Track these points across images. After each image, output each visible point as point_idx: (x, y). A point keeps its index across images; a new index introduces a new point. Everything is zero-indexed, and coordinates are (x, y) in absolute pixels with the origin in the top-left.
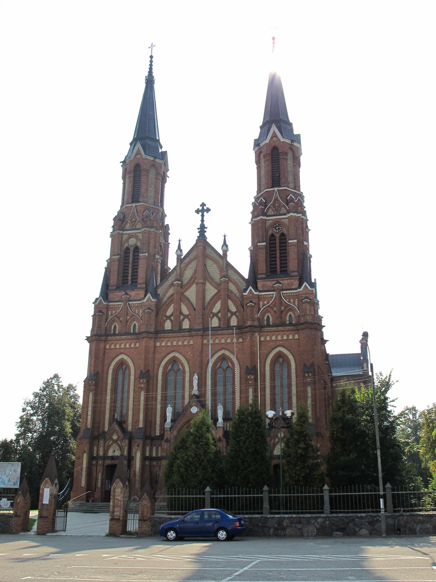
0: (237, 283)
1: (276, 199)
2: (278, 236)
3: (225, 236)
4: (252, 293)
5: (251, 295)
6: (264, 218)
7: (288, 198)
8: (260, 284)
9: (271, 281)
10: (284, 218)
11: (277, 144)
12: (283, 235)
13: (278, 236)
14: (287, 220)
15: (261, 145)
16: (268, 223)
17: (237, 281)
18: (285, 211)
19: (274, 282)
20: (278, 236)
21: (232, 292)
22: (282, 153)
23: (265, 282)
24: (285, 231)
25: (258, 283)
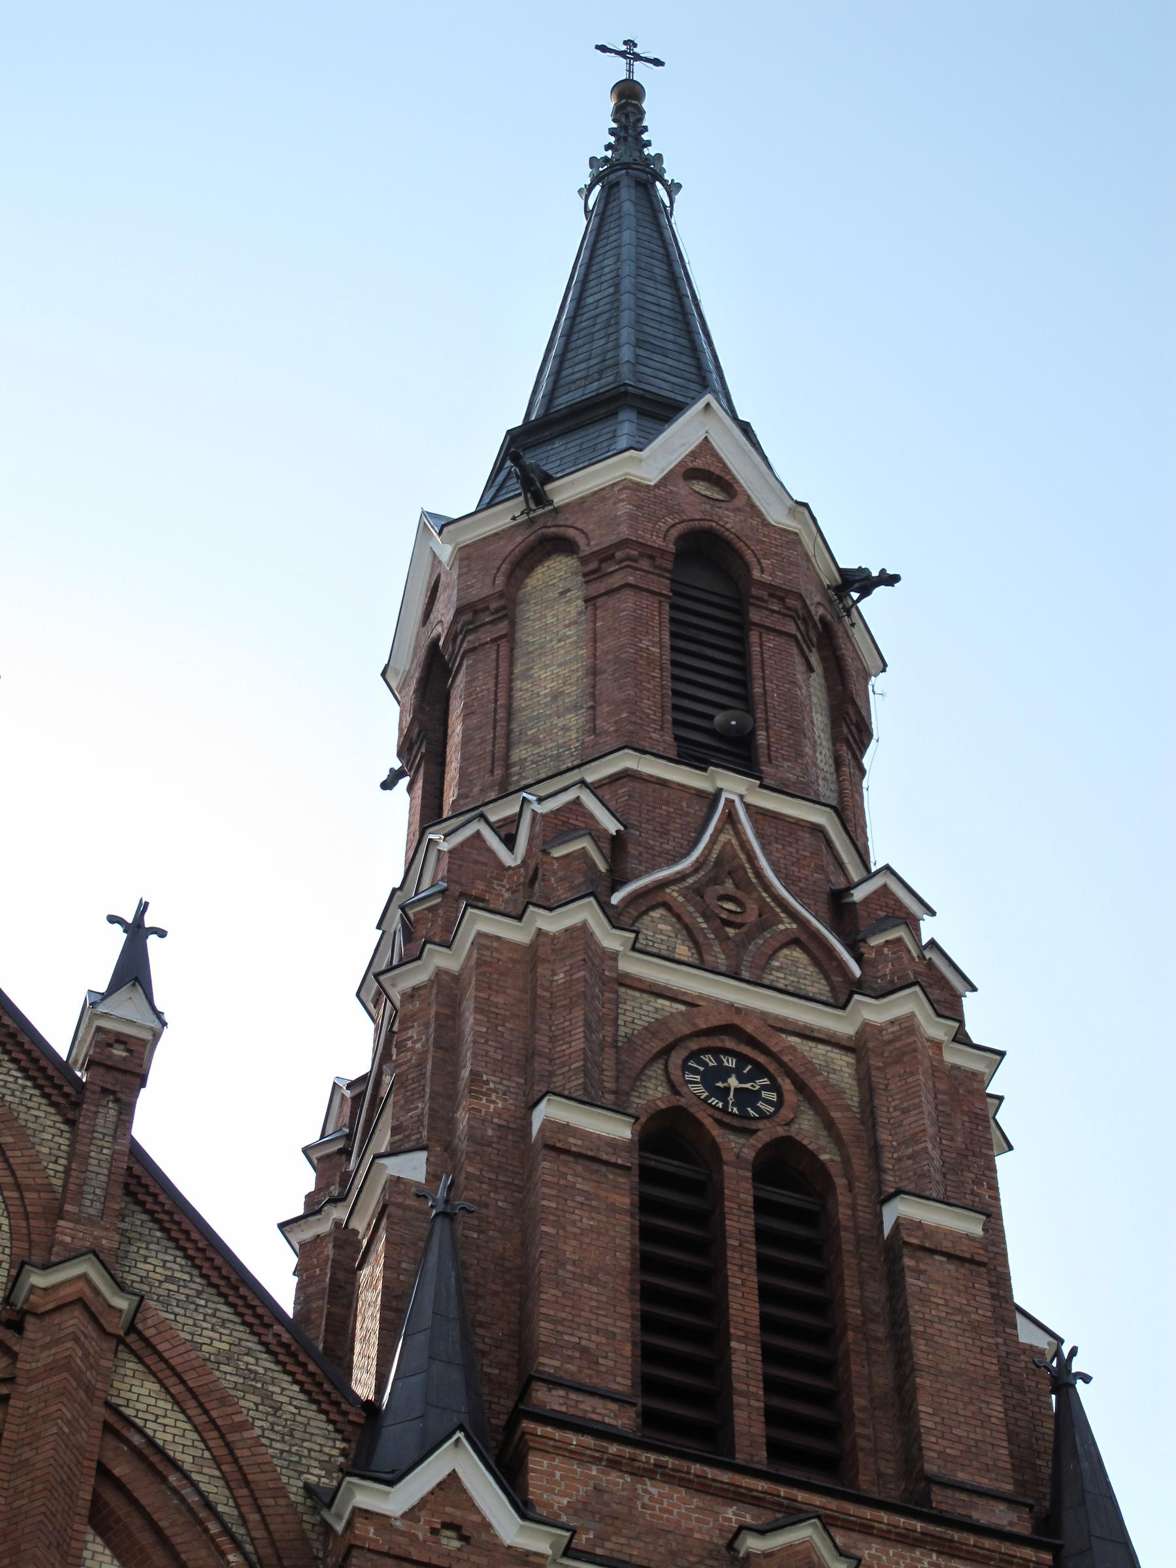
0: (224, 1400)
1: (728, 868)
2: (738, 1150)
3: (137, 933)
4: (469, 1529)
5: (451, 1542)
6: (611, 940)
7: (858, 895)
8: (552, 1475)
9: (702, 1487)
10: (807, 1034)
11: (730, 522)
12: (783, 1165)
13: (738, 1150)
14: (842, 1062)
15: (564, 492)
16: (639, 1012)
17: (227, 1377)
18: (819, 987)
19: (731, 1514)
20: (749, 1154)
21: (154, 1460)
22: (777, 593)
23: (618, 1481)
24: (806, 1128)
25: (537, 1464)
